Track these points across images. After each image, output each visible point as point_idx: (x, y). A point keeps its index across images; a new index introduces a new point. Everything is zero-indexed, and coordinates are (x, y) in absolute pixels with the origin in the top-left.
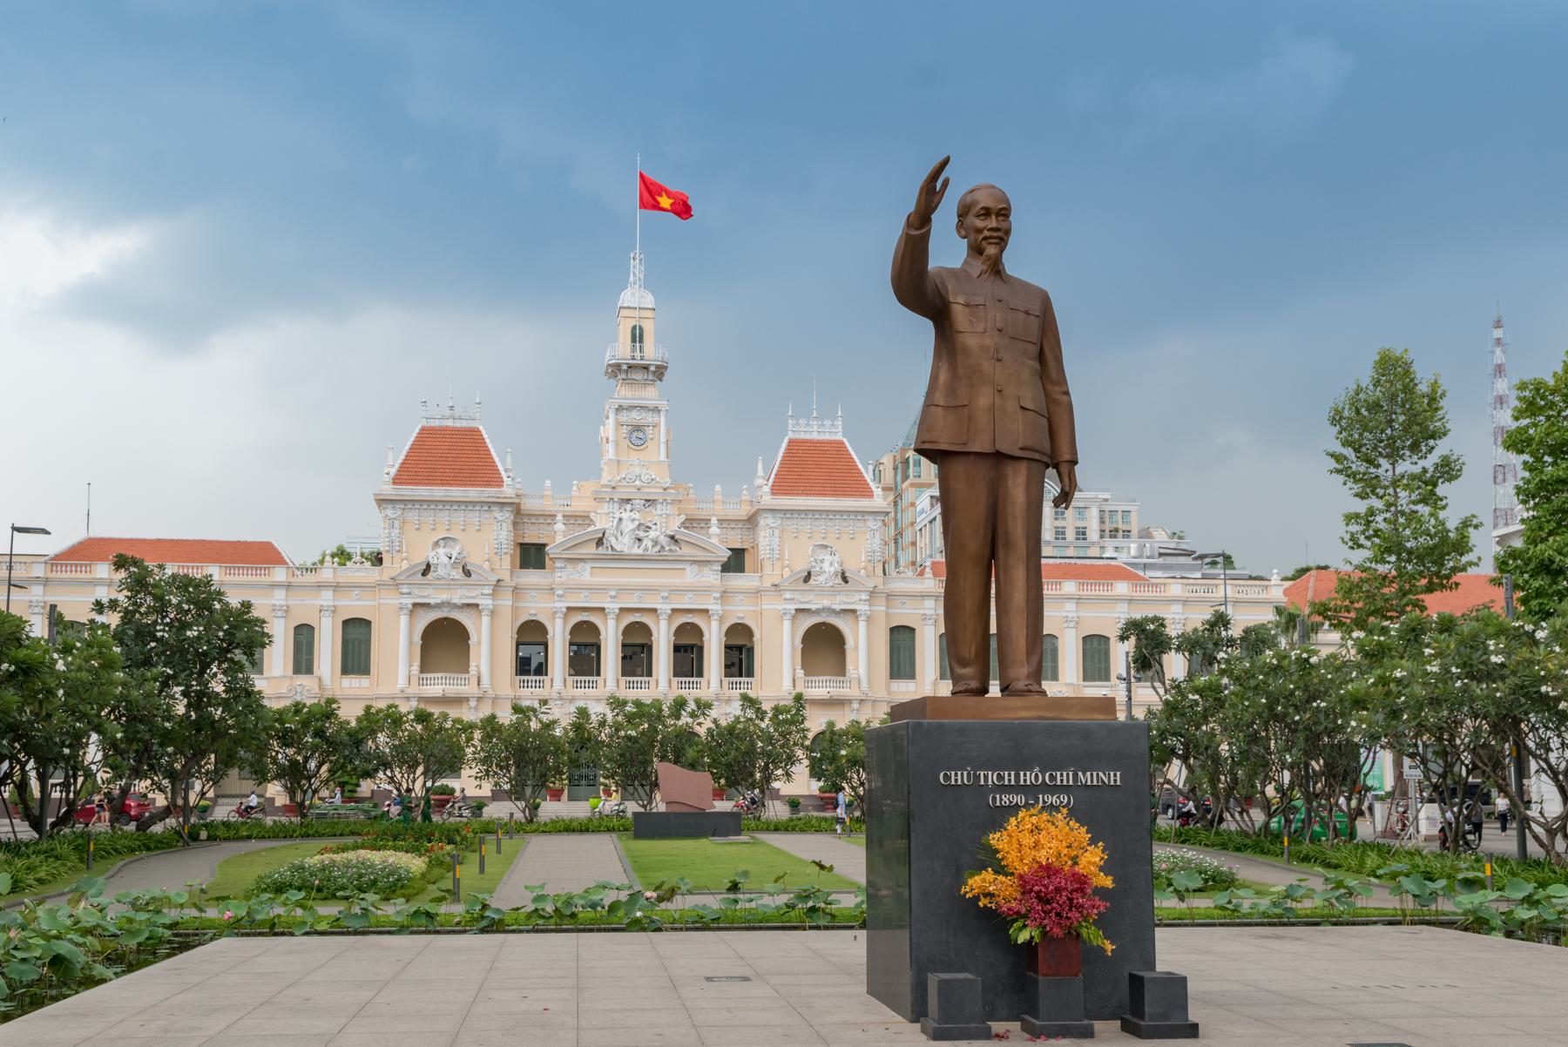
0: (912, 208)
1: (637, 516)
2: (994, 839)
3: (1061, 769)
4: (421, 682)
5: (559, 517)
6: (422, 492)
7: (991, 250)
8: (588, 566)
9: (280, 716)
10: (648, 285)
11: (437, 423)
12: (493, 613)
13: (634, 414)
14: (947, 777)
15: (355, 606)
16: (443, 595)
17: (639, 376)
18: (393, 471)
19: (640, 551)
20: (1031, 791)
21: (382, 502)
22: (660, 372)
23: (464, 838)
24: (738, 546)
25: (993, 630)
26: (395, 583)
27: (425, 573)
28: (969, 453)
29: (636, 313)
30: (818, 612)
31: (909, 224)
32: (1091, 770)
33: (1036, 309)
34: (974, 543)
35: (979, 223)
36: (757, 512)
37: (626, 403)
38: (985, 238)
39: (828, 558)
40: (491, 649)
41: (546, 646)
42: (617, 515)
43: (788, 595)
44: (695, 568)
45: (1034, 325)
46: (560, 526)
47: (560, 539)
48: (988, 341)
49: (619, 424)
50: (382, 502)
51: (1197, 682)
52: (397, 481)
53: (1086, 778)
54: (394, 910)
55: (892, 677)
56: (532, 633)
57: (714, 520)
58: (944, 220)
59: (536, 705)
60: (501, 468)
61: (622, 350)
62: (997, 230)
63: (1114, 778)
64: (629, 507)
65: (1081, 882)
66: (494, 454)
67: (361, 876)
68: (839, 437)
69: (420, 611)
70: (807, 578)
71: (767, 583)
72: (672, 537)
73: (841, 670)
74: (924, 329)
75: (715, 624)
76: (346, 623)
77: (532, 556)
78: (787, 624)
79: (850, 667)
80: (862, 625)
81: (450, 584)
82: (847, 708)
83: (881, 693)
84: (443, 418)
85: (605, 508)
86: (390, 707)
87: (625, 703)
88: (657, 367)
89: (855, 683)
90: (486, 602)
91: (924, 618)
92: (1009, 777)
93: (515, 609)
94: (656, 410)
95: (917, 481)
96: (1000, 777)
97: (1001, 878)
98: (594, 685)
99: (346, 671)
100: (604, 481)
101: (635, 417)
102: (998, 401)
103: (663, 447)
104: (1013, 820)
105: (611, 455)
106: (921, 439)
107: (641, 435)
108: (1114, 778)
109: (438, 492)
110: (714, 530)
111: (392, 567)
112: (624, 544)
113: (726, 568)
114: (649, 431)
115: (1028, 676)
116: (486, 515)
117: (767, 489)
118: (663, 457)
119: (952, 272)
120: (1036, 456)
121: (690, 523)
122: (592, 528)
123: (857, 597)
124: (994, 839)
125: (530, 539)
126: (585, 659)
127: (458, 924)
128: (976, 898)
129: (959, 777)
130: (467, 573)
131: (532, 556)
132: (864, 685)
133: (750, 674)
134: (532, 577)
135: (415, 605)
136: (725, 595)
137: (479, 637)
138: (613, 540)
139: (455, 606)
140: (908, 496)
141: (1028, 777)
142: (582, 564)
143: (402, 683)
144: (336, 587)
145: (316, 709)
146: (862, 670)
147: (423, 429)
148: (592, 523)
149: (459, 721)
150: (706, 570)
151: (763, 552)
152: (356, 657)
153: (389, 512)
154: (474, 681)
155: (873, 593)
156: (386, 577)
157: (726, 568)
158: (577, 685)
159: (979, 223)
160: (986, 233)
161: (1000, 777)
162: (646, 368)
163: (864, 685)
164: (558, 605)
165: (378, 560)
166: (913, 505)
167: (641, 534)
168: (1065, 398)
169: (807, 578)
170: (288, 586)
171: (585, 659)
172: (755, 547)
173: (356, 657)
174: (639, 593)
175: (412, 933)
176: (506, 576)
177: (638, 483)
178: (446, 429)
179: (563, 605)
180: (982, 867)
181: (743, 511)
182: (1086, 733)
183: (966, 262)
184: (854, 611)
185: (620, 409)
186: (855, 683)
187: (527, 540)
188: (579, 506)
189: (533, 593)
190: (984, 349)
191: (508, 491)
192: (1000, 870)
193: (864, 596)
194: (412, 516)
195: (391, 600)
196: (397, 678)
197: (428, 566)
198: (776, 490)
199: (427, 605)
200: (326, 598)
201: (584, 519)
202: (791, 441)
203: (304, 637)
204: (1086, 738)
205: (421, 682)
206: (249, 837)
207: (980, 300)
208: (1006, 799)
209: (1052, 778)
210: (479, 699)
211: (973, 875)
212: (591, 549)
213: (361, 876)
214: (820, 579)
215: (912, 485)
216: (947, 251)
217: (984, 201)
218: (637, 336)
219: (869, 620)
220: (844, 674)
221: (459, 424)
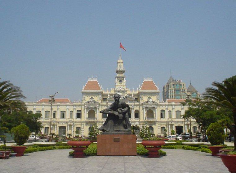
13: (120, 78)
15: (79, 108)
30: (149, 108)
52: (85, 89)
61: (119, 69)
75: (133, 110)
78: (144, 110)
79: (154, 116)
81: (93, 105)
101: (121, 79)
117: (140, 89)
125: (105, 97)
139: (93, 108)
162: (122, 71)
197: (89, 102)
198: (142, 89)
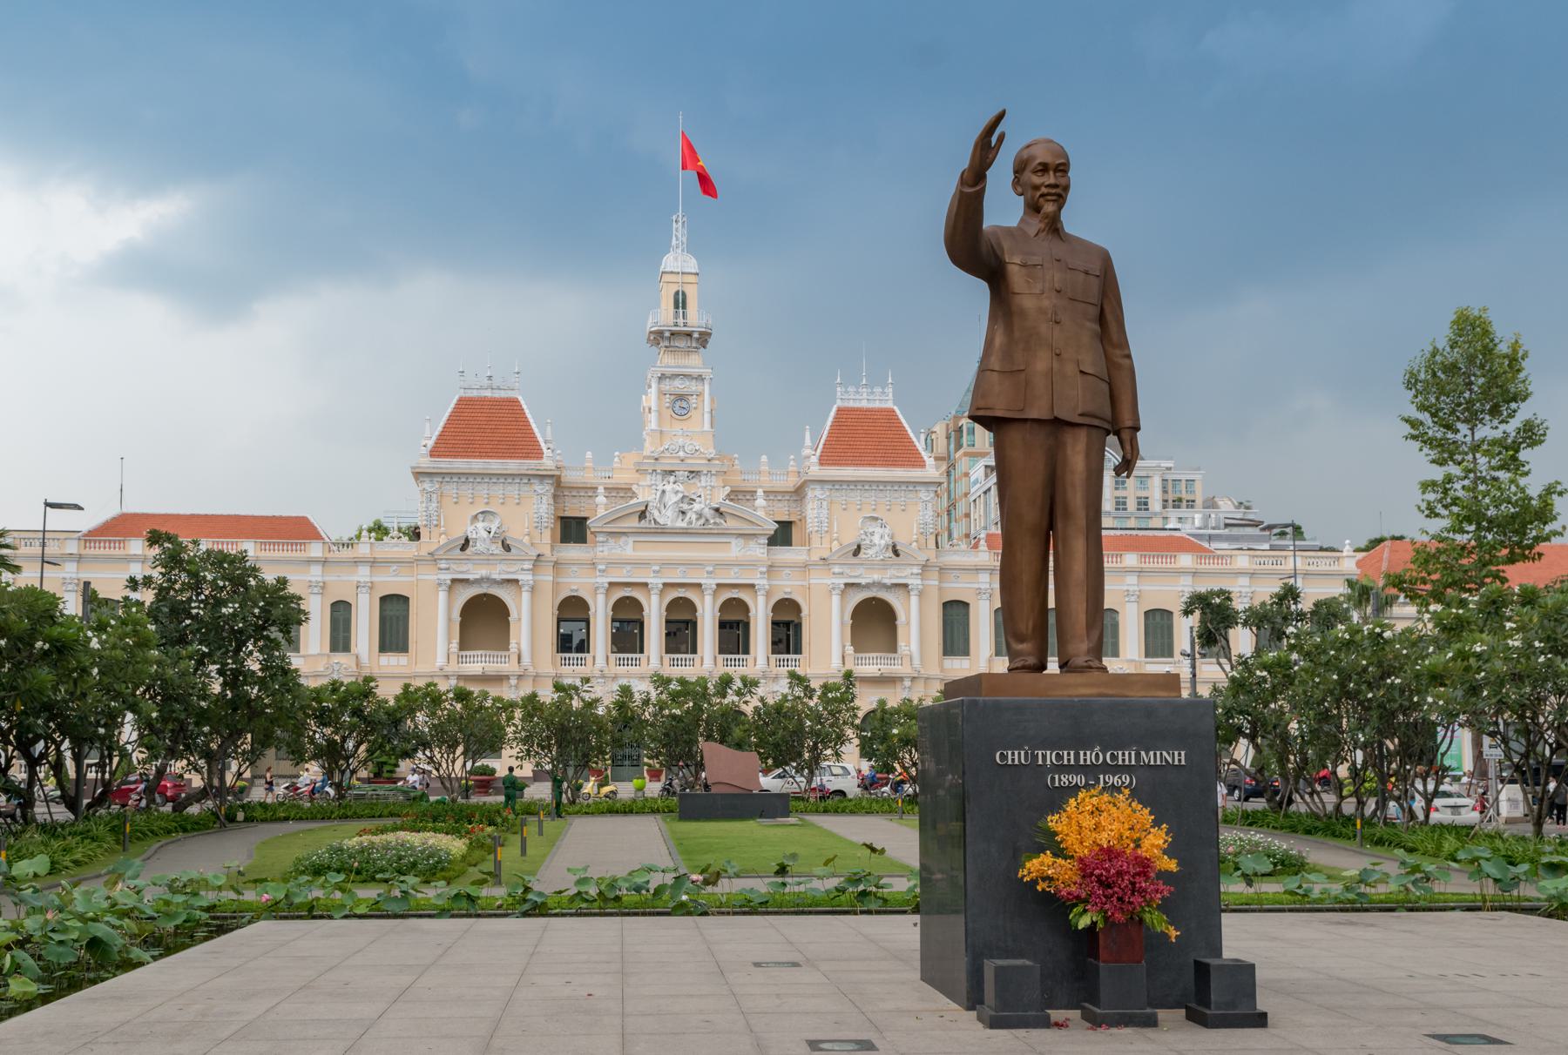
0: (965, 164)
1: (680, 488)
2: (1053, 821)
3: (1123, 748)
4: (460, 659)
5: (601, 490)
6: (460, 464)
7: (1049, 208)
8: (631, 540)
9: (317, 694)
10: (692, 248)
11: (474, 394)
12: (533, 589)
13: (677, 383)
14: (1003, 757)
15: (392, 582)
16: (482, 570)
17: (681, 343)
18: (431, 443)
19: (684, 525)
20: (1091, 771)
21: (419, 475)
22: (704, 339)
23: (505, 820)
24: (785, 518)
25: (1051, 604)
26: (433, 558)
27: (464, 547)
28: (1026, 420)
29: (679, 278)
30: (868, 586)
31: (963, 181)
32: (1155, 750)
33: (1096, 268)
34: (1032, 514)
35: (1037, 180)
36: (806, 482)
37: (669, 371)
38: (1042, 195)
39: (878, 530)
40: (531, 625)
41: (588, 622)
42: (660, 488)
43: (837, 569)
44: (741, 541)
45: (1095, 284)
46: (601, 499)
47: (601, 512)
48: (1046, 303)
49: (662, 393)
50: (419, 475)
51: (1265, 658)
52: (435, 453)
53: (1149, 758)
54: (434, 893)
55: (945, 654)
56: (573, 610)
57: (760, 492)
58: (1000, 175)
59: (578, 683)
60: (540, 439)
61: (664, 316)
62: (1056, 186)
63: (1179, 757)
64: (672, 479)
65: (1144, 865)
66: (534, 426)
67: (400, 858)
68: (890, 405)
69: (459, 587)
70: (857, 552)
71: (815, 557)
72: (717, 510)
73: (892, 646)
74: (979, 291)
75: (761, 600)
76: (383, 599)
77: (573, 529)
78: (836, 599)
79: (901, 643)
80: (914, 600)
81: (489, 559)
82: (898, 686)
83: (934, 671)
84: (481, 388)
85: (648, 480)
86: (428, 685)
87: (669, 681)
88: (701, 333)
89: (906, 661)
90: (525, 577)
91: (979, 592)
92: (1068, 757)
93: (556, 585)
94: (700, 378)
95: (971, 450)
96: (1059, 757)
97: (1059, 861)
98: (637, 663)
99: (384, 647)
100: (646, 452)
101: (679, 385)
102: (1056, 365)
103: (707, 417)
104: (1072, 801)
105: (653, 425)
106: (975, 406)
107: (684, 404)
108: (1179, 757)
109: (477, 465)
110: (760, 502)
111: (429, 543)
112: (667, 518)
113: (773, 541)
114: (693, 400)
115: (1089, 652)
116: (526, 488)
117: (814, 459)
118: (707, 427)
119: (1009, 231)
120: (1096, 422)
121: (735, 495)
122: (634, 501)
123: (908, 571)
124: (1053, 821)
126: (627, 636)
127: (500, 907)
128: (1034, 882)
129: (1016, 757)
130: (507, 548)
131: (573, 529)
132: (916, 662)
133: (798, 651)
134: (573, 551)
135: (454, 581)
136: (771, 569)
137: (519, 613)
138: (656, 513)
139: (495, 582)
140: (962, 465)
141: (1088, 757)
142: (623, 539)
143: (440, 660)
144: (373, 563)
145: (353, 688)
146: (914, 647)
147: (460, 400)
148: (634, 496)
149: (497, 699)
150: (752, 544)
151: (811, 525)
152: (393, 635)
153: (427, 486)
154: (514, 659)
155: (925, 567)
156: (424, 552)
157: (773, 541)
158: (620, 662)
159: (1037, 180)
160: (1044, 190)
161: (1059, 757)
162: (689, 335)
163: (916, 662)
164: (600, 580)
165: (415, 534)
166: (967, 475)
167: (685, 507)
168: (1127, 361)
169: (857, 552)
170: (324, 562)
171: (627, 636)
172: (803, 519)
173: (393, 635)
174: (682, 568)
175: (453, 916)
176: (546, 551)
177: (681, 454)
178: (483, 400)
179: (605, 580)
180: (1041, 850)
181: (791, 482)
182: (1149, 710)
183: (1022, 220)
184: (906, 586)
185: (662, 378)
186: (906, 661)
187: (567, 514)
188: (621, 478)
189: (575, 568)
190: (1042, 311)
191: (547, 463)
192: (1059, 853)
193: (916, 570)
194: (451, 489)
195: (430, 576)
196: (436, 655)
197: (467, 540)
198: (823, 461)
199: (466, 581)
200: (363, 574)
201: (626, 491)
202: (839, 410)
203: (341, 613)
204: (1151, 716)
205: (460, 659)
206: (286, 819)
207: (1036, 260)
208: (1065, 780)
209: (1114, 757)
210: (520, 677)
211: (1030, 859)
212: (633, 523)
213: (400, 858)
214: (870, 552)
215: (966, 454)
216: (1003, 209)
217: (1042, 156)
218: (680, 302)
219: (921, 594)
220: (895, 651)
221: (498, 394)
